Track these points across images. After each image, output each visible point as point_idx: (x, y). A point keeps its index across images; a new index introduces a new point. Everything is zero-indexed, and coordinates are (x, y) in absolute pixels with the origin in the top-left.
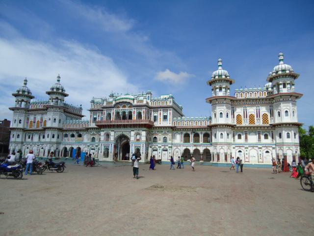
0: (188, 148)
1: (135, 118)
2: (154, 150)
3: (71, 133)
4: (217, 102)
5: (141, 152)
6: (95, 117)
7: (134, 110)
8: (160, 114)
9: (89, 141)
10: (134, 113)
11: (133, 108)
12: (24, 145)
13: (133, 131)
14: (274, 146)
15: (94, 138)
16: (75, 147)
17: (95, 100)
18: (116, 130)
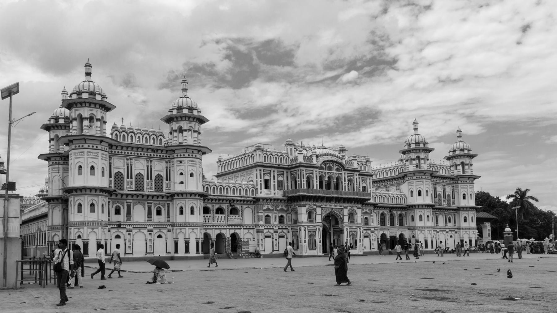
3: (217, 206)
4: (424, 177)
6: (267, 177)
7: (344, 175)
8: (360, 185)
10: (345, 181)
11: (343, 172)
14: (456, 230)
15: (267, 216)
17: (262, 146)
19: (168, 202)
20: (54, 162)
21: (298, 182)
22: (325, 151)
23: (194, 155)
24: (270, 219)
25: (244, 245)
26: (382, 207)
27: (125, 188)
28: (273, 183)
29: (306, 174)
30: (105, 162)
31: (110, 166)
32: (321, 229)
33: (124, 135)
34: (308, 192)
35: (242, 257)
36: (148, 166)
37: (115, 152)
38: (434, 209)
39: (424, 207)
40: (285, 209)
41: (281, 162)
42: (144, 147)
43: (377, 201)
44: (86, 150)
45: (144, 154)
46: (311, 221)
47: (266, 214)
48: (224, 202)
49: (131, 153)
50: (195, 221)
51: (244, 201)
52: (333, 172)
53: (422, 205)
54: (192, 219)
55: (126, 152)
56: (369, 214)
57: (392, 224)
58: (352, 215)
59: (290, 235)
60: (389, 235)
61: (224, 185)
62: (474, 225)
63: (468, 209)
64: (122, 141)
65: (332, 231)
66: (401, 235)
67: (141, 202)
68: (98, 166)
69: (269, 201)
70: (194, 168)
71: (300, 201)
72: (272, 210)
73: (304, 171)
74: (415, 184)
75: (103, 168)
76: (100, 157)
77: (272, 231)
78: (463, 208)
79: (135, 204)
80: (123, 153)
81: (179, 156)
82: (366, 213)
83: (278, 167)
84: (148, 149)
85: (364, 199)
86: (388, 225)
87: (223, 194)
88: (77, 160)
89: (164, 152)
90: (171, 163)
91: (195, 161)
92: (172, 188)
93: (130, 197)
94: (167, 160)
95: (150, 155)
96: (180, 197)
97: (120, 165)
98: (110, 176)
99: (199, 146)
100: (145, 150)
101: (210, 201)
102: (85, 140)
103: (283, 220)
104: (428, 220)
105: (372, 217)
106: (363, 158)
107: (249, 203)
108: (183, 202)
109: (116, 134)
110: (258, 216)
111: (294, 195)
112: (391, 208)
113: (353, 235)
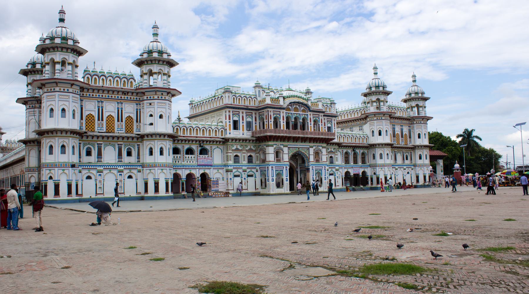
3: (187, 147)
4: (383, 118)
6: (236, 118)
7: (310, 116)
10: (311, 122)
11: (309, 113)
12: (80, 172)
13: (312, 147)
14: (413, 167)
15: (236, 156)
16: (197, 173)
19: (138, 143)
20: (31, 106)
21: (265, 123)
22: (292, 93)
23: (163, 97)
24: (239, 159)
25: (214, 184)
26: (346, 146)
27: (96, 130)
28: (242, 124)
30: (76, 105)
31: (82, 109)
32: (288, 168)
33: (95, 78)
34: (275, 132)
35: (211, 197)
36: (118, 108)
37: (86, 95)
38: (393, 148)
39: (384, 146)
40: (254, 149)
41: (250, 104)
42: (114, 89)
43: (342, 141)
44: (57, 93)
45: (115, 97)
46: (279, 161)
47: (235, 154)
48: (194, 142)
49: (102, 96)
50: (164, 161)
51: (213, 142)
52: (299, 113)
53: (382, 144)
54: (161, 160)
55: (98, 94)
56: (334, 153)
57: (355, 162)
58: (317, 154)
59: (258, 174)
60: (352, 172)
61: (194, 126)
62: (427, 162)
63: (423, 148)
64: (93, 84)
65: (299, 170)
66: (364, 173)
67: (112, 143)
68: (69, 109)
69: (238, 141)
70: (164, 110)
71: (268, 141)
72: (241, 150)
73: (271, 112)
74: (375, 125)
75: (74, 110)
76: (71, 100)
77: (241, 171)
78: (418, 146)
79: (106, 145)
80: (94, 96)
81: (149, 98)
82: (331, 152)
83: (247, 108)
84: (118, 92)
85: (328, 139)
86: (352, 163)
87: (192, 135)
88: (49, 103)
89: (135, 94)
90: (142, 105)
91: (164, 103)
92: (142, 130)
93: (100, 139)
94: (137, 102)
95: (121, 97)
96: (150, 138)
97: (91, 107)
98: (82, 118)
99: (169, 89)
100: (115, 93)
101: (180, 142)
102: (57, 83)
103: (252, 159)
104: (388, 158)
105: (336, 156)
106: (328, 100)
107: (218, 143)
108: (153, 143)
109: (88, 78)
110: (227, 156)
111: (262, 135)
112: (354, 148)
113: (319, 173)
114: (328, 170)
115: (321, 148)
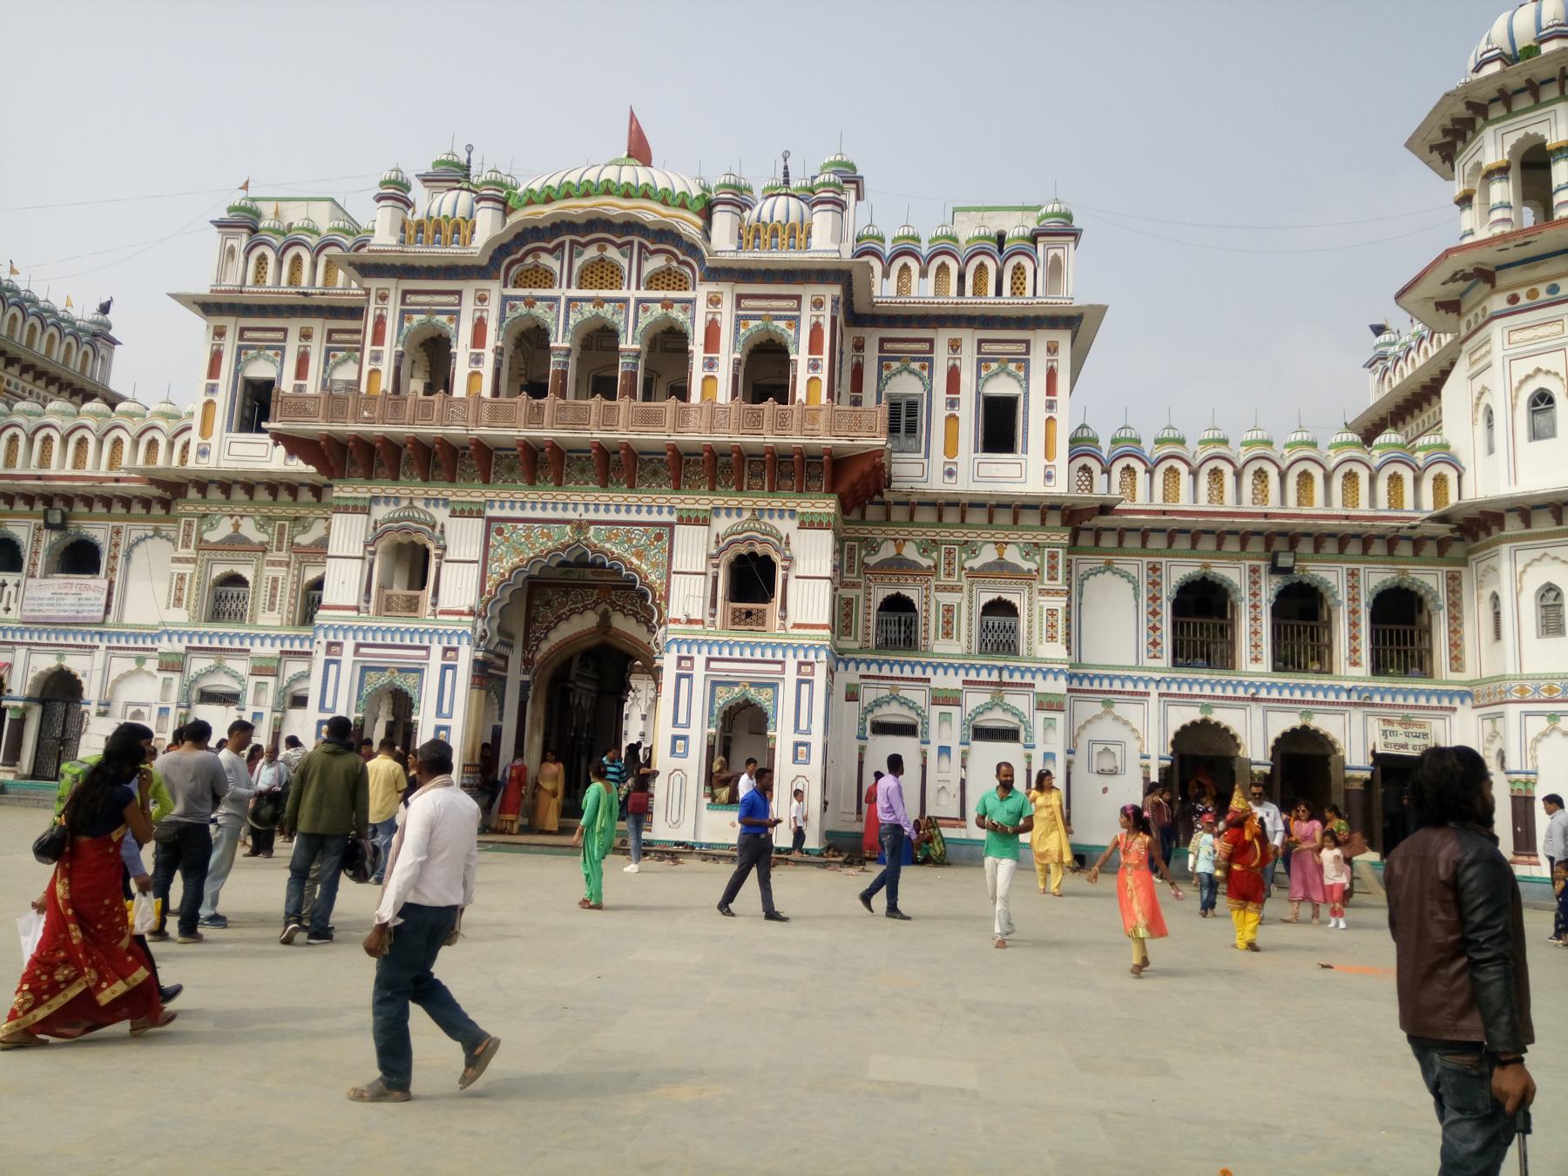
0: (1220, 716)
1: (723, 394)
2: (882, 728)
5: (782, 736)
6: (260, 370)
8: (953, 383)
9: (180, 616)
10: (712, 342)
11: (702, 292)
15: (236, 580)
17: (267, 209)
18: (514, 501)
29: (404, 315)
32: (466, 657)
47: (219, 571)
56: (1027, 577)
72: (263, 548)
77: (241, 666)
112: (1276, 542)
114: (852, 696)
115: (787, 526)
